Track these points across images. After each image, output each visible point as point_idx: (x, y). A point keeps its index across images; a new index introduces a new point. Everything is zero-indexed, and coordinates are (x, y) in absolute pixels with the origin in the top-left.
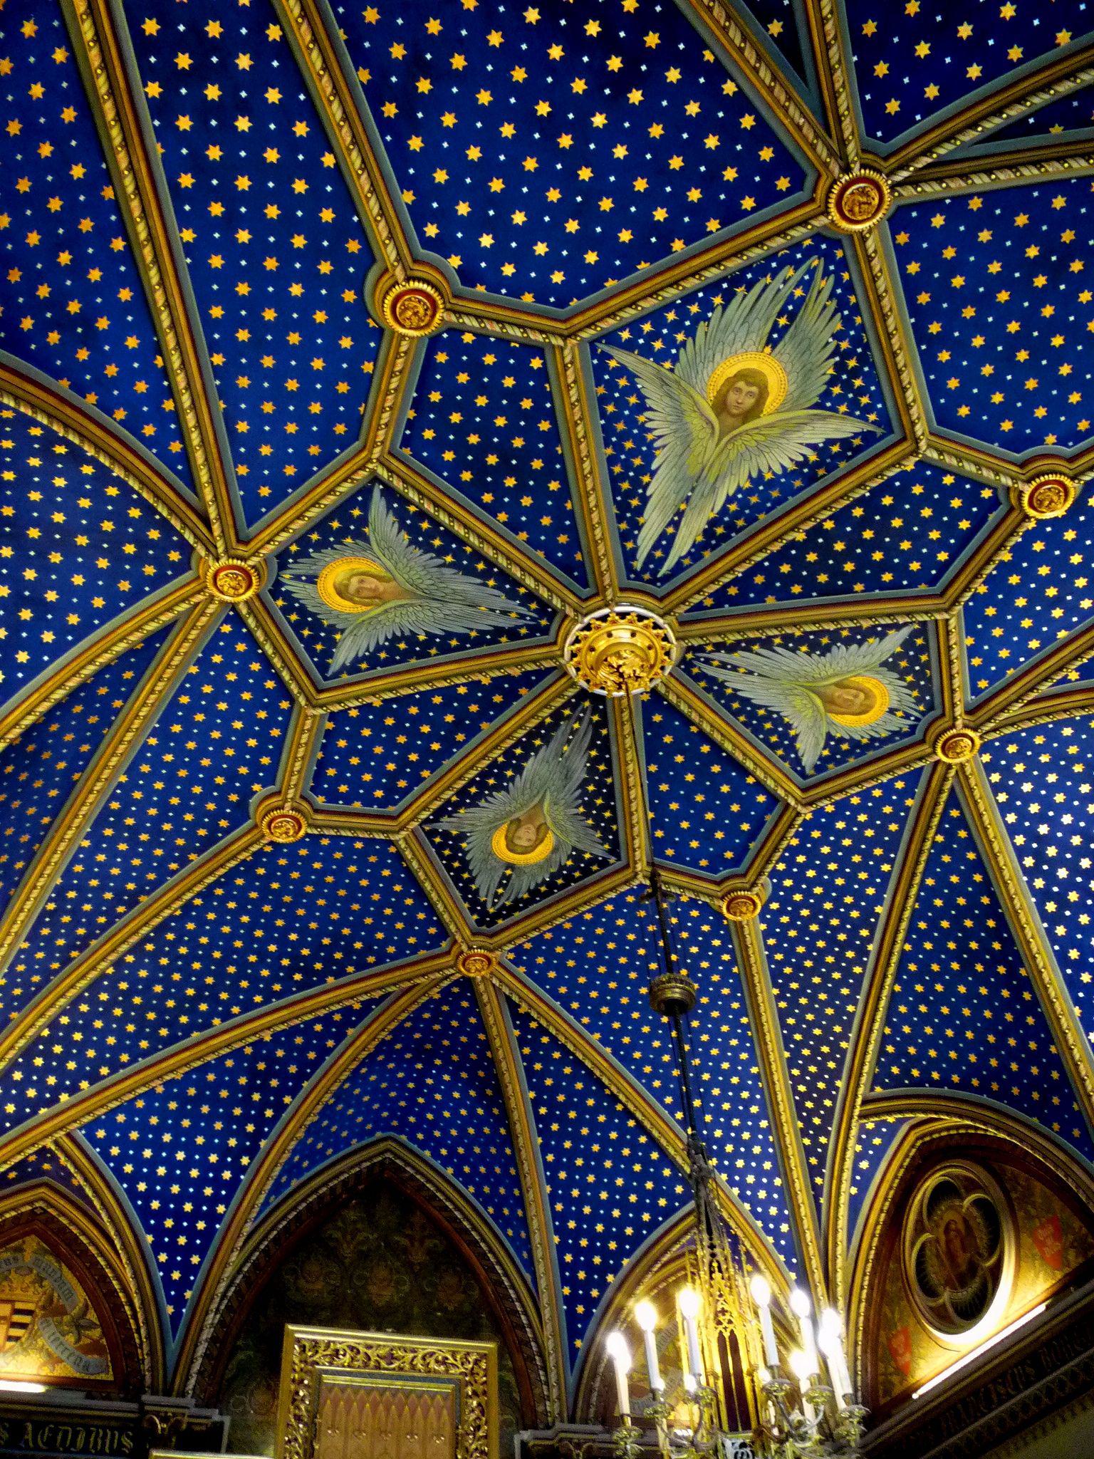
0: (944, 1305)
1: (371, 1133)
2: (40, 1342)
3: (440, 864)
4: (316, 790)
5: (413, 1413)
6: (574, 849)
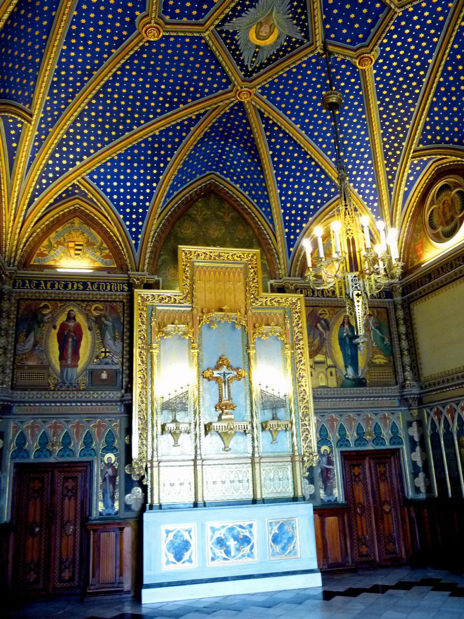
0: (438, 233)
1: (205, 172)
2: (87, 255)
3: (226, 47)
4: (165, 13)
5: (229, 275)
6: (287, 36)
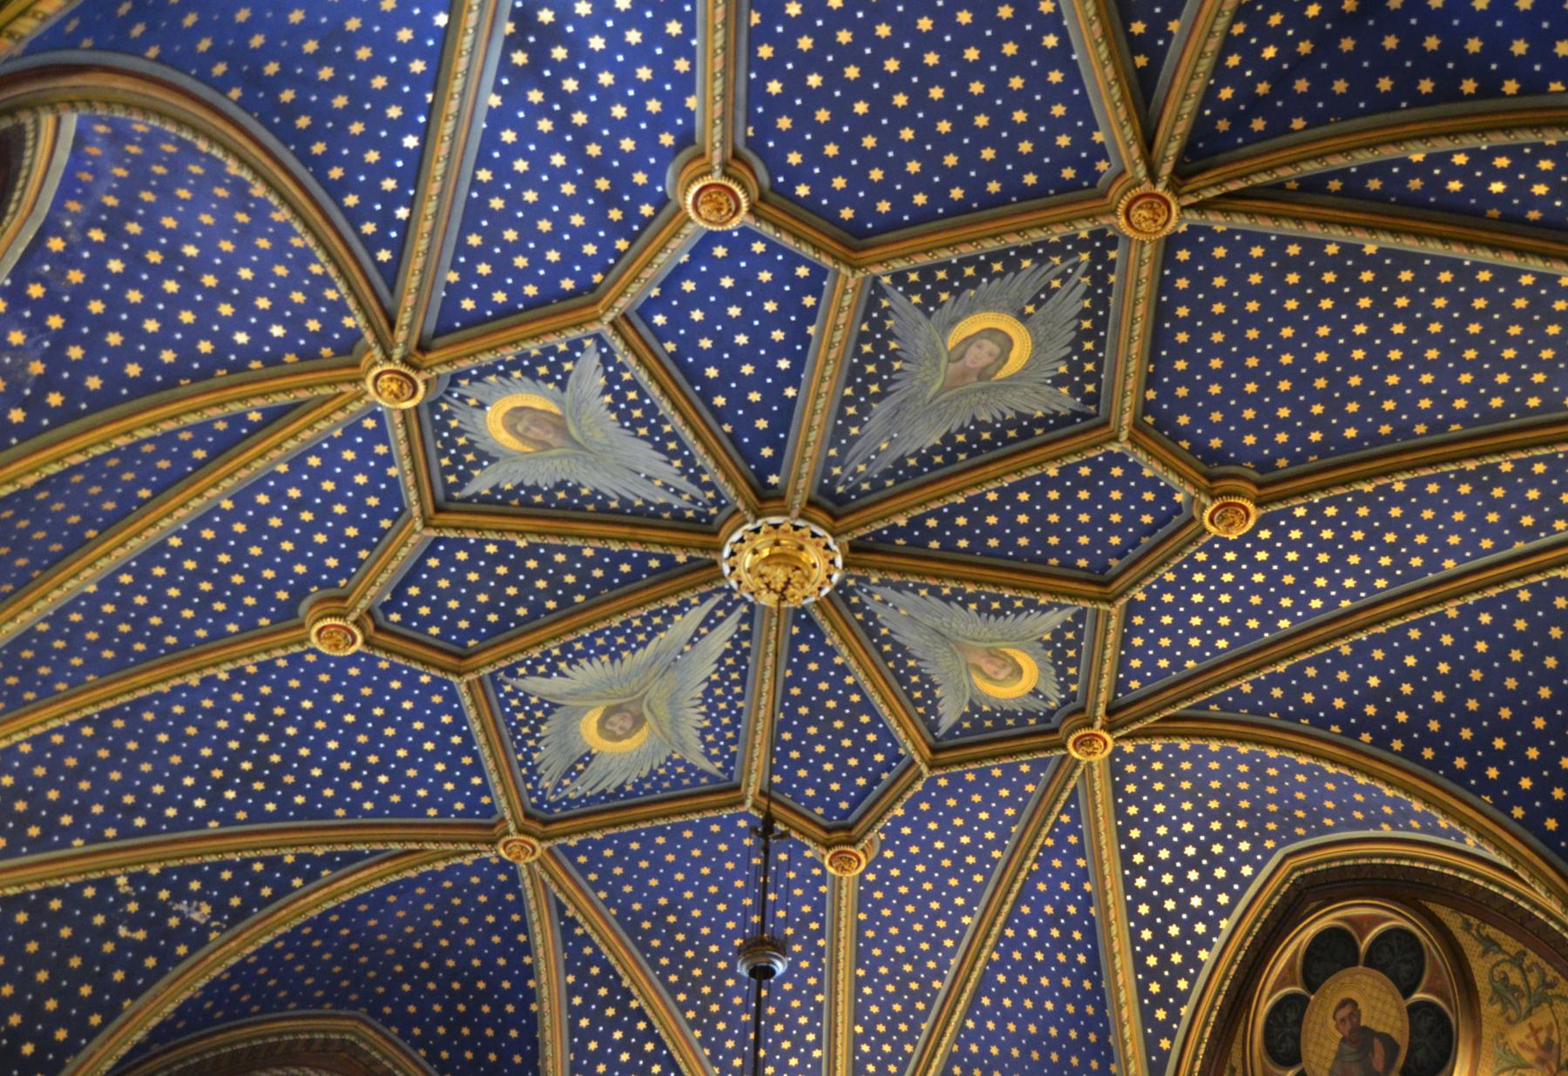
6: (929, 315)
